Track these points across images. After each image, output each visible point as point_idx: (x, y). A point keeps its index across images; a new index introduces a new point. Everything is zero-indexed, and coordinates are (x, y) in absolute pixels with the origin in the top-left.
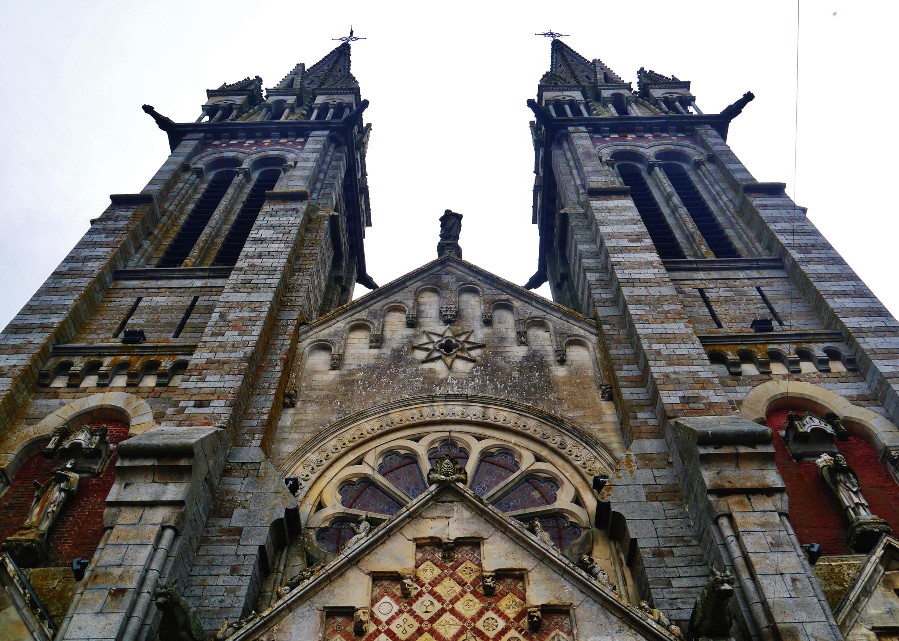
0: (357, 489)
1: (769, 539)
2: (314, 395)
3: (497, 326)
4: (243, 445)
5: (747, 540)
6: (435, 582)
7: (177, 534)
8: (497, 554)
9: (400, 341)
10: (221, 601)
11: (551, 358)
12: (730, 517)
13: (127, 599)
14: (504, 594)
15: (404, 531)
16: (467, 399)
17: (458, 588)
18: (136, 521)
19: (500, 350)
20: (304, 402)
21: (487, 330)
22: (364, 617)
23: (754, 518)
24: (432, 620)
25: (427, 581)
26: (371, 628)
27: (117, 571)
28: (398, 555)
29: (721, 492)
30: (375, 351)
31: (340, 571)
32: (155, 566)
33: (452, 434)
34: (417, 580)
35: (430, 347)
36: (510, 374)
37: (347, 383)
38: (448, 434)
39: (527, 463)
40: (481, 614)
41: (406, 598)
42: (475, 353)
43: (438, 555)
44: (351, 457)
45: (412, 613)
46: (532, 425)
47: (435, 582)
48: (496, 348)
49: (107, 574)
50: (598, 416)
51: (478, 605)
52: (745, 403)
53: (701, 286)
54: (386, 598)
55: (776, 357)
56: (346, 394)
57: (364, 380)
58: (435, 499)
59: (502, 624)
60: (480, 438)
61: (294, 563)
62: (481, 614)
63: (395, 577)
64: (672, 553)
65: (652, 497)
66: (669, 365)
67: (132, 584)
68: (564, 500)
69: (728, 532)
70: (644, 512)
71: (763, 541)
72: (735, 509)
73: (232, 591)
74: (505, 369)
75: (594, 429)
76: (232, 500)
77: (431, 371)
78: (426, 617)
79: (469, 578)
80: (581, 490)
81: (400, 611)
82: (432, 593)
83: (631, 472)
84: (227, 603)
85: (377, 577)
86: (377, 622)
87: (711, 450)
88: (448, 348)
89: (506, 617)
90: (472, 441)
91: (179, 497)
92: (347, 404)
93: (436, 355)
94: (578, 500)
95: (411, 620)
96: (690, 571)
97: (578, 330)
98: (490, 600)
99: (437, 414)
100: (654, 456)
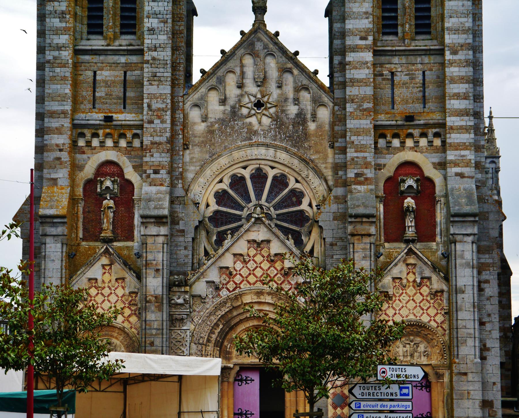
0: (221, 197)
1: (363, 255)
2: (197, 140)
3: (284, 87)
4: (175, 187)
5: (356, 255)
6: (254, 256)
7: (167, 244)
8: (276, 247)
9: (234, 99)
10: (184, 260)
11: (309, 116)
12: (353, 244)
13: (161, 272)
14: (277, 261)
15: (243, 237)
16: (267, 146)
17: (262, 259)
18: (153, 242)
19: (284, 109)
20: (192, 146)
21: (279, 91)
22: (232, 270)
23: (361, 246)
24: (254, 270)
25: (251, 256)
26: (234, 273)
27: (154, 262)
28: (242, 247)
29: (353, 235)
30: (222, 108)
31: (223, 254)
32: (165, 259)
33: (261, 166)
34: (248, 255)
35: (249, 105)
36: (288, 128)
37: (210, 131)
38: (258, 166)
39: (292, 184)
40: (269, 268)
41: (245, 262)
43: (255, 245)
44: (218, 179)
45: (247, 267)
46: (296, 162)
47: (254, 256)
48: (283, 107)
49: (152, 264)
50: (326, 157)
51: (269, 265)
52: (387, 166)
53: (394, 70)
54: (238, 262)
55: (410, 135)
56: (211, 140)
57: (220, 129)
58: (254, 223)
59: (276, 272)
60: (272, 168)
61: (202, 233)
62: (269, 268)
63: (241, 255)
64: (336, 244)
65: (335, 219)
66: (356, 152)
67: (160, 267)
68: (304, 206)
69: (351, 250)
70: (330, 226)
71: (361, 256)
72: (356, 242)
73: (186, 256)
74: (286, 124)
75: (322, 166)
76: (177, 216)
77: (250, 124)
78: (252, 269)
79: (266, 255)
80: (312, 200)
81: (243, 267)
82: (253, 260)
83: (330, 206)
84: (186, 261)
85: (235, 255)
86: (236, 271)
87: (353, 220)
88: (259, 105)
89: (277, 270)
90: (269, 169)
91: (166, 233)
92: (213, 147)
93: (253, 112)
94: (310, 205)
95: (247, 269)
96: (341, 252)
98: (272, 263)
99: (254, 155)
100: (341, 197)
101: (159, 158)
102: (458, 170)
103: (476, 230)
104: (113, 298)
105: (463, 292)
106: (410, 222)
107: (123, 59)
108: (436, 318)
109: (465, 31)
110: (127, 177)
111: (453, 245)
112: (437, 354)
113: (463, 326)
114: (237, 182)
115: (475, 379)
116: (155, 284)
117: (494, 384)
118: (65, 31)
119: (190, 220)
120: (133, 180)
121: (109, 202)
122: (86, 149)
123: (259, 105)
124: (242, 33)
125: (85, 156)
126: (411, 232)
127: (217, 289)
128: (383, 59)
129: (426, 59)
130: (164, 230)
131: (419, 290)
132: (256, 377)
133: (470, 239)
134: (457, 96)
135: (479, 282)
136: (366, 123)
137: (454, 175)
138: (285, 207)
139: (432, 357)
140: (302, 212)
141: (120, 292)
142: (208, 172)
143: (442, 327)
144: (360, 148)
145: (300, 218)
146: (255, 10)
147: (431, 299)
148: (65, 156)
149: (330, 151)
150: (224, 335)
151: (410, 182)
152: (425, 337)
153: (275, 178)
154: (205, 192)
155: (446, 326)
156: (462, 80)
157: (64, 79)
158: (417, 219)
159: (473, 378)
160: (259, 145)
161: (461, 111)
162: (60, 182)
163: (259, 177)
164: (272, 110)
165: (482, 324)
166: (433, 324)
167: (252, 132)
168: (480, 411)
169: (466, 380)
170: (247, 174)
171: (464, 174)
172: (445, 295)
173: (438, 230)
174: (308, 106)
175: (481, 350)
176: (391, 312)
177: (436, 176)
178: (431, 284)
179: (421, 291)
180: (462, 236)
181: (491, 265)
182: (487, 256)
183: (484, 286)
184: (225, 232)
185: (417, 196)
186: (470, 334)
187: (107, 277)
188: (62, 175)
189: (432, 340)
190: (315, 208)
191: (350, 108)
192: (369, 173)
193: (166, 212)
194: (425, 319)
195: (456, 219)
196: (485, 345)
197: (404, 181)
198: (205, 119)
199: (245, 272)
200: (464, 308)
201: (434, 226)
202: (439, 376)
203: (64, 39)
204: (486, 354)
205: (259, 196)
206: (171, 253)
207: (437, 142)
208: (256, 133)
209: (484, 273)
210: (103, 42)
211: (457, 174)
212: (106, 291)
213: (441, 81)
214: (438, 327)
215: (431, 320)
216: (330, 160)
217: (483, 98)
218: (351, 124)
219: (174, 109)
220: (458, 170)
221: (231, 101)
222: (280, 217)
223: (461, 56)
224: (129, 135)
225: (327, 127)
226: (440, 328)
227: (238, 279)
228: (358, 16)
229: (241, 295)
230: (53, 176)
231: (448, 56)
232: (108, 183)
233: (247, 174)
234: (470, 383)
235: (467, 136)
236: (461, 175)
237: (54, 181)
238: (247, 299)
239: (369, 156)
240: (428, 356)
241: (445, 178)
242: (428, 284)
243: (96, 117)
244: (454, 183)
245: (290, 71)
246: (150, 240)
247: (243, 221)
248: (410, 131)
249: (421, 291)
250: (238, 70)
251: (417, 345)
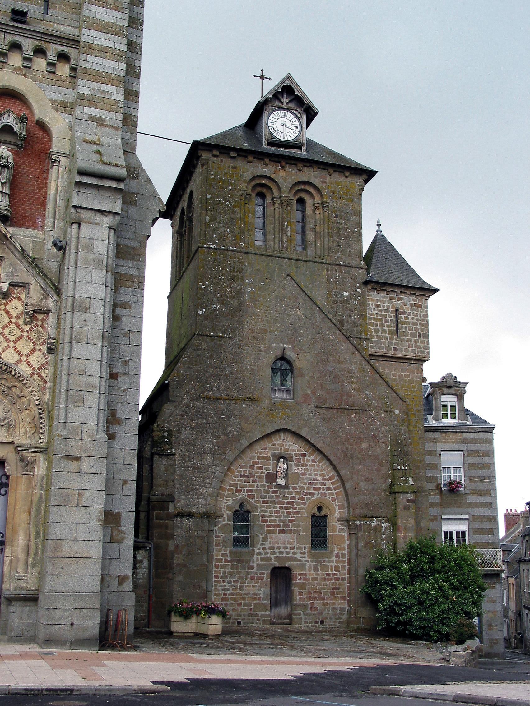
103: (118, 207)
105: (86, 310)
108: (31, 359)
111: (75, 226)
112: (26, 424)
113: (81, 370)
115: (93, 470)
117: (125, 482)
131: (5, 305)
133: (107, 220)
135: (115, 305)
137: (86, 117)
139: (17, 430)
143: (40, 376)
147: (26, 323)
155: (47, 374)
159: (91, 467)
161: (107, 24)
165: (113, 376)
166: (24, 369)
168: (100, 529)
169: (76, 470)
171: (104, 120)
173: (49, 211)
175: (109, 422)
178: (28, 296)
179: (8, 307)
180: (92, 213)
181: (135, 280)
182: (129, 263)
183: (119, 311)
186: (93, 386)
189: (20, 398)
195: (86, 180)
196: (113, 414)
200: (85, 338)
202: (27, 465)
204: (114, 429)
209: (122, 290)
211: (92, 119)
214: (33, 374)
215: (21, 361)
217: (142, 24)
226: (36, 376)
234: (85, 476)
235: (114, 64)
236: (100, 122)
240: (8, 428)
242: (23, 296)
248: (17, 38)
249: (8, 307)
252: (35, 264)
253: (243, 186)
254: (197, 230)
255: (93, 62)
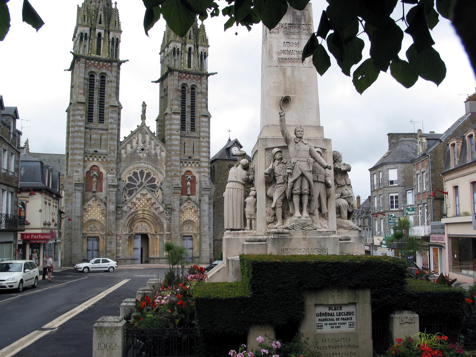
0: (130, 179)
8: (149, 196)
16: (145, 163)
28: (139, 196)
39: (152, 176)
41: (139, 200)
42: (147, 152)
46: (154, 169)
50: (163, 167)
55: (190, 162)
68: (156, 183)
75: (162, 170)
97: (164, 149)
101: (113, 165)
102: (203, 174)
104: (96, 211)
106: (189, 189)
107: (101, 132)
109: (206, 132)
110: (101, 171)
114: (135, 174)
116: (112, 207)
118: (82, 121)
119: (123, 185)
120: (103, 172)
121: (94, 179)
122: (87, 161)
123: (143, 150)
124: (138, 126)
125: (87, 163)
126: (189, 193)
127: (131, 209)
128: (182, 138)
129: (194, 140)
130: (115, 189)
132: (140, 237)
133: (207, 195)
134: (204, 152)
136: (178, 158)
138: (151, 183)
140: (155, 185)
141: (99, 209)
142: (126, 171)
144: (176, 166)
145: (154, 187)
146: (142, 119)
148: (82, 163)
149: (165, 166)
150: (131, 223)
151: (189, 177)
152: (192, 225)
153: (147, 173)
154: (125, 177)
155: (198, 221)
156: (205, 147)
157: (81, 137)
158: (191, 189)
160: (142, 163)
162: (79, 172)
163: (142, 173)
164: (147, 152)
166: (195, 221)
167: (140, 159)
170: (138, 171)
172: (199, 212)
173: (196, 192)
174: (159, 152)
176: (183, 217)
177: (197, 176)
184: (133, 190)
185: (191, 181)
187: (94, 204)
188: (80, 169)
190: (160, 184)
191: (173, 153)
192: (178, 174)
193: (117, 184)
194: (193, 219)
197: (187, 177)
198: (126, 153)
199: (139, 204)
201: (195, 191)
202: (196, 236)
203: (82, 124)
205: (142, 179)
206: (117, 197)
207: (197, 165)
208: (141, 159)
210: (94, 125)
212: (94, 209)
213: (200, 147)
216: (165, 168)
218: (173, 158)
219: (118, 149)
220: (203, 174)
221: (134, 147)
222: (148, 186)
223: (205, 140)
224: (102, 157)
225: (164, 158)
227: (137, 206)
228: (175, 124)
229: (138, 211)
230: (77, 170)
231: (201, 139)
232: (95, 173)
233: (138, 171)
236: (205, 176)
237: (78, 172)
238: (139, 212)
239: (179, 169)
241: (200, 177)
243: (92, 150)
244: (203, 179)
245: (153, 139)
246: (111, 193)
247: (137, 187)
250: (137, 139)
251: (190, 227)
252: (196, 204)
253: (226, 167)
254: (216, 178)
255: (203, 164)
